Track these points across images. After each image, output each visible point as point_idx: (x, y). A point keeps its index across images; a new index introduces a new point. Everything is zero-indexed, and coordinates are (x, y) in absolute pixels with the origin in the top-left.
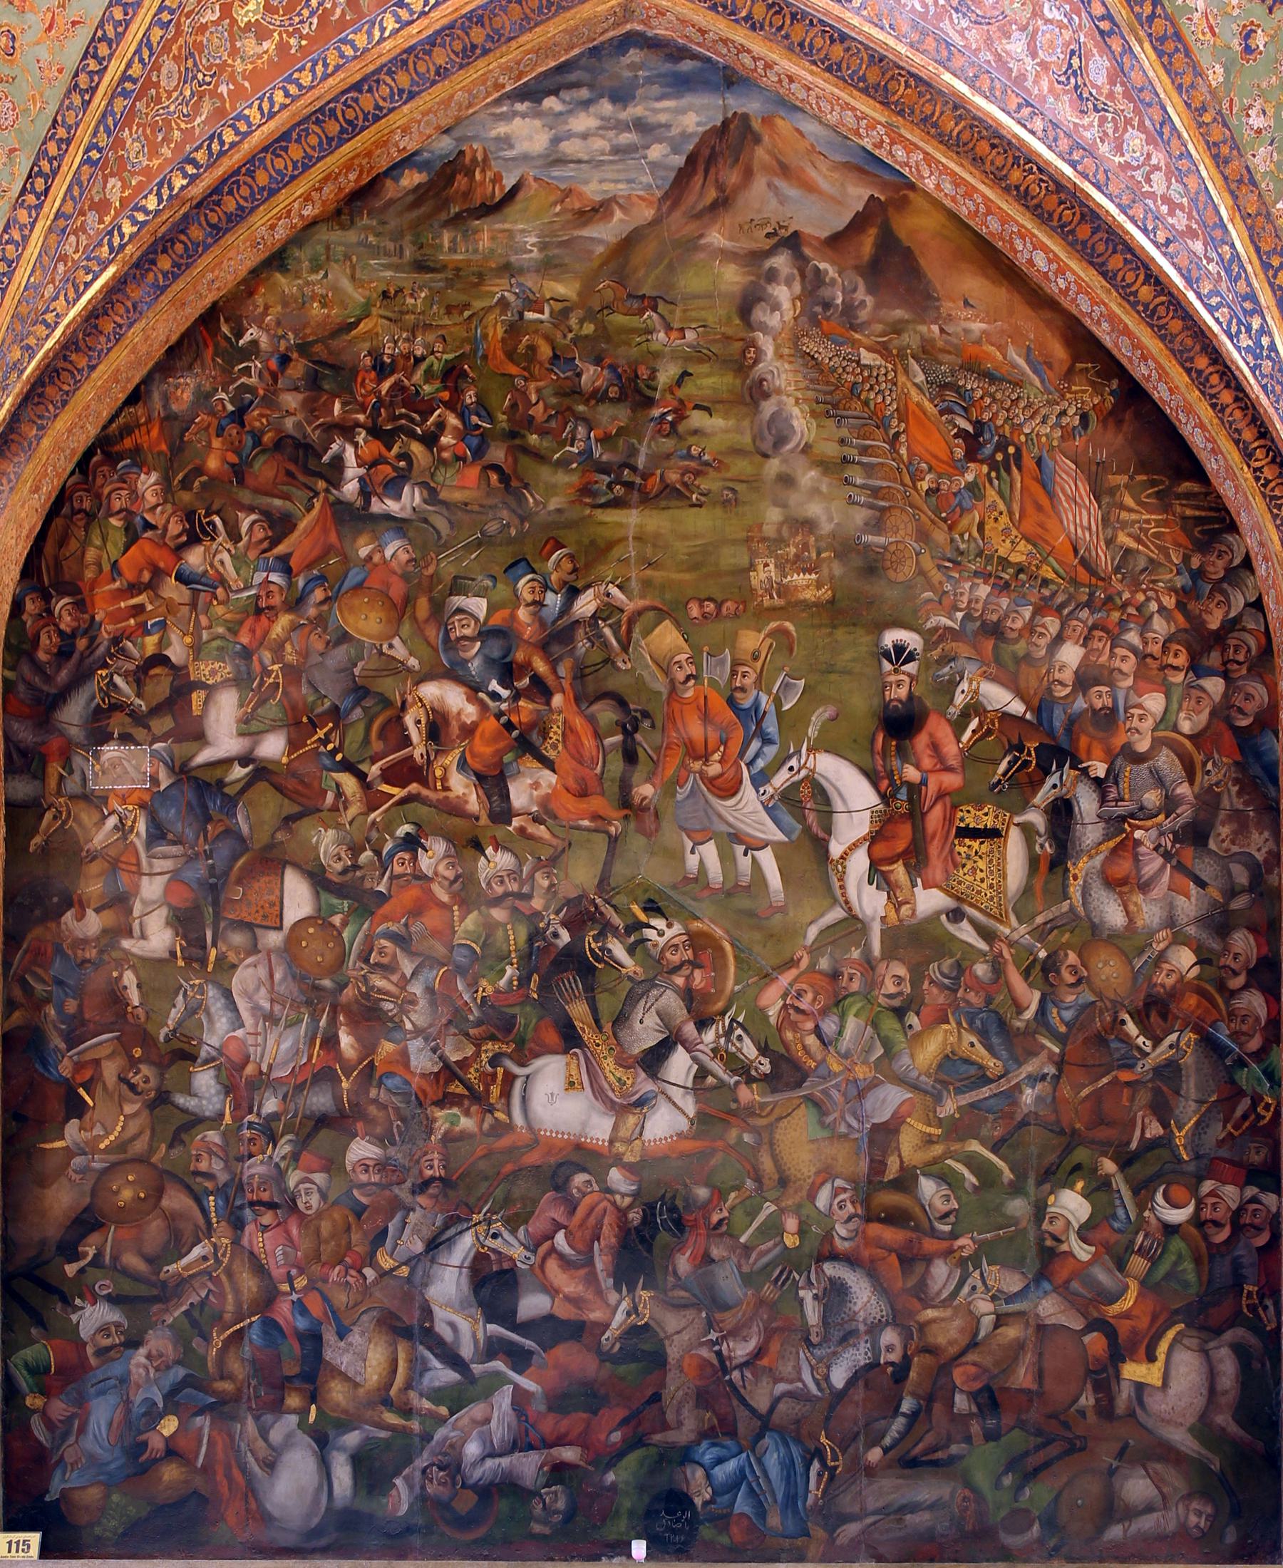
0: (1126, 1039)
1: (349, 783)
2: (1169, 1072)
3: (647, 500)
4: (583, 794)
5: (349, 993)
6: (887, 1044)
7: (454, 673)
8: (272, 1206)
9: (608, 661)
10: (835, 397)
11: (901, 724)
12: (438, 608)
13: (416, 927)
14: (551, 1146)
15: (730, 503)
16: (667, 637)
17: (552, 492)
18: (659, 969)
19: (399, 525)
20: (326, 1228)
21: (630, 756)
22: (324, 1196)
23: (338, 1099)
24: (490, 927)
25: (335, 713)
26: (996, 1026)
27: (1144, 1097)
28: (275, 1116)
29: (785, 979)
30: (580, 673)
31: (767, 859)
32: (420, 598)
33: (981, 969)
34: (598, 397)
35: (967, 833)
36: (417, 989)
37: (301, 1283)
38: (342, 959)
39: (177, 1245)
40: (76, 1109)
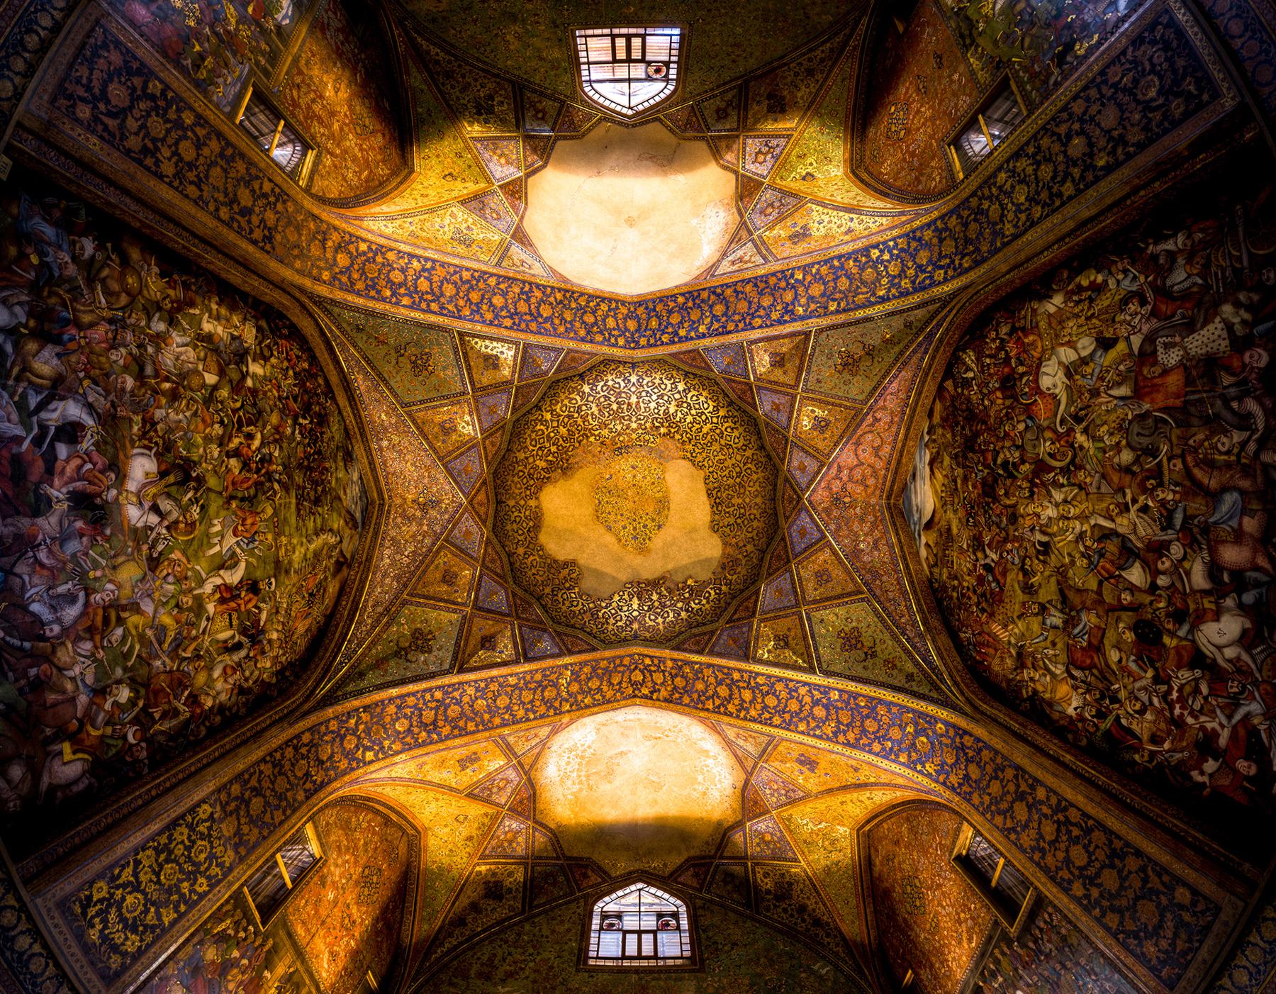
0: (183, 692)
1: (238, 405)
2: (176, 713)
3: (297, 504)
4: (234, 483)
5: (182, 390)
6: (167, 602)
7: (262, 444)
8: (115, 338)
9: (265, 493)
10: (317, 555)
11: (254, 588)
12: (276, 441)
13: (199, 419)
14: (125, 464)
15: (297, 529)
16: (270, 511)
17: (299, 478)
18: (185, 510)
19: (293, 433)
20: (103, 359)
21: (243, 499)
22: (115, 362)
23: (148, 377)
24: (198, 447)
25: (254, 405)
26: (178, 643)
27: (166, 707)
28: (146, 350)
29: (184, 560)
30: (262, 484)
31: (217, 548)
32: (278, 437)
33: (194, 632)
34: (316, 491)
35: (230, 615)
36: (181, 416)
37: (83, 342)
38: (192, 390)
39: (108, 293)
40: (162, 275)
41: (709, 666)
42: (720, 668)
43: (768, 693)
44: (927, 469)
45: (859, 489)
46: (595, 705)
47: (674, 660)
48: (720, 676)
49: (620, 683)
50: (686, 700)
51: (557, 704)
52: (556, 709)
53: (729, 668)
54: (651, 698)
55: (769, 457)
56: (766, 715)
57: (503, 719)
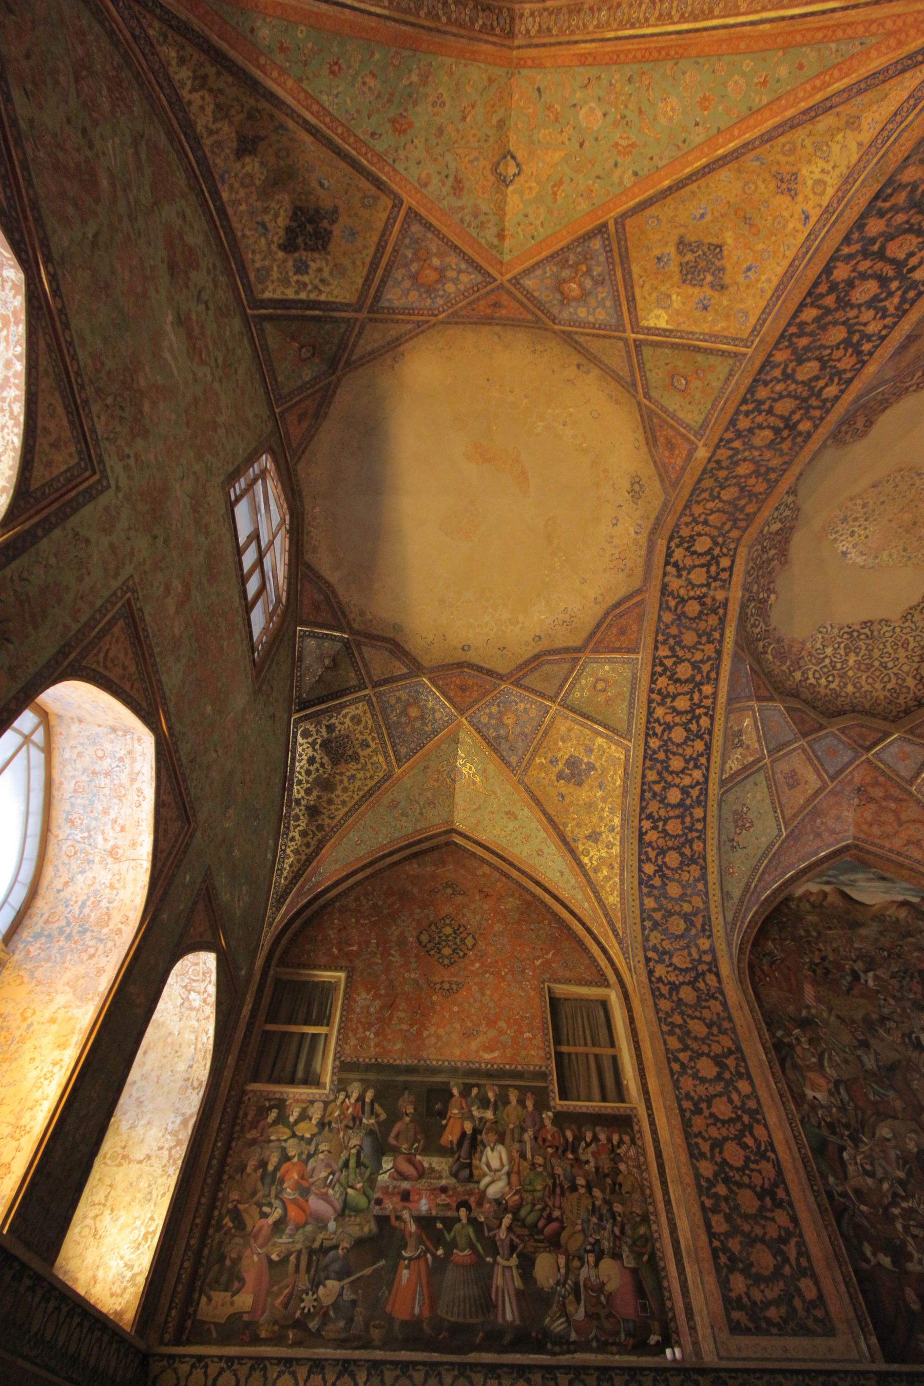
41: (719, 652)
42: (717, 668)
43: (688, 730)
44: (900, 898)
45: (868, 816)
46: (694, 490)
47: (725, 605)
48: (706, 668)
49: (706, 523)
50: (668, 617)
51: (737, 444)
52: (731, 441)
53: (717, 679)
54: (667, 563)
55: (907, 712)
56: (659, 729)
57: (776, 366)
